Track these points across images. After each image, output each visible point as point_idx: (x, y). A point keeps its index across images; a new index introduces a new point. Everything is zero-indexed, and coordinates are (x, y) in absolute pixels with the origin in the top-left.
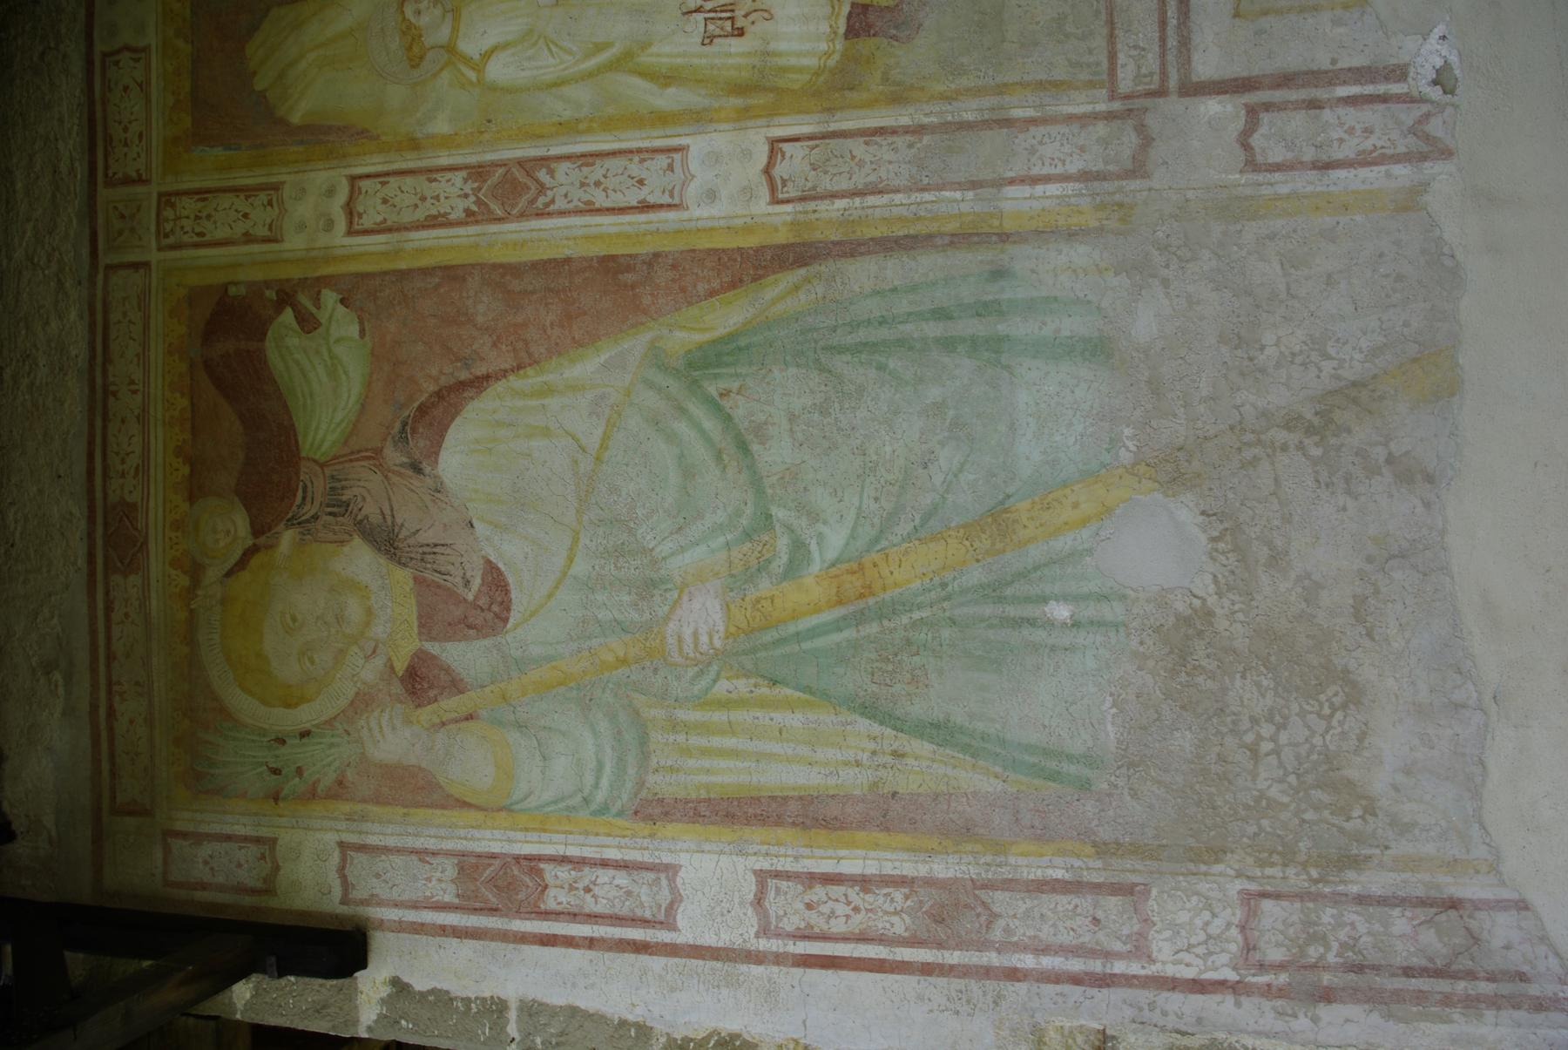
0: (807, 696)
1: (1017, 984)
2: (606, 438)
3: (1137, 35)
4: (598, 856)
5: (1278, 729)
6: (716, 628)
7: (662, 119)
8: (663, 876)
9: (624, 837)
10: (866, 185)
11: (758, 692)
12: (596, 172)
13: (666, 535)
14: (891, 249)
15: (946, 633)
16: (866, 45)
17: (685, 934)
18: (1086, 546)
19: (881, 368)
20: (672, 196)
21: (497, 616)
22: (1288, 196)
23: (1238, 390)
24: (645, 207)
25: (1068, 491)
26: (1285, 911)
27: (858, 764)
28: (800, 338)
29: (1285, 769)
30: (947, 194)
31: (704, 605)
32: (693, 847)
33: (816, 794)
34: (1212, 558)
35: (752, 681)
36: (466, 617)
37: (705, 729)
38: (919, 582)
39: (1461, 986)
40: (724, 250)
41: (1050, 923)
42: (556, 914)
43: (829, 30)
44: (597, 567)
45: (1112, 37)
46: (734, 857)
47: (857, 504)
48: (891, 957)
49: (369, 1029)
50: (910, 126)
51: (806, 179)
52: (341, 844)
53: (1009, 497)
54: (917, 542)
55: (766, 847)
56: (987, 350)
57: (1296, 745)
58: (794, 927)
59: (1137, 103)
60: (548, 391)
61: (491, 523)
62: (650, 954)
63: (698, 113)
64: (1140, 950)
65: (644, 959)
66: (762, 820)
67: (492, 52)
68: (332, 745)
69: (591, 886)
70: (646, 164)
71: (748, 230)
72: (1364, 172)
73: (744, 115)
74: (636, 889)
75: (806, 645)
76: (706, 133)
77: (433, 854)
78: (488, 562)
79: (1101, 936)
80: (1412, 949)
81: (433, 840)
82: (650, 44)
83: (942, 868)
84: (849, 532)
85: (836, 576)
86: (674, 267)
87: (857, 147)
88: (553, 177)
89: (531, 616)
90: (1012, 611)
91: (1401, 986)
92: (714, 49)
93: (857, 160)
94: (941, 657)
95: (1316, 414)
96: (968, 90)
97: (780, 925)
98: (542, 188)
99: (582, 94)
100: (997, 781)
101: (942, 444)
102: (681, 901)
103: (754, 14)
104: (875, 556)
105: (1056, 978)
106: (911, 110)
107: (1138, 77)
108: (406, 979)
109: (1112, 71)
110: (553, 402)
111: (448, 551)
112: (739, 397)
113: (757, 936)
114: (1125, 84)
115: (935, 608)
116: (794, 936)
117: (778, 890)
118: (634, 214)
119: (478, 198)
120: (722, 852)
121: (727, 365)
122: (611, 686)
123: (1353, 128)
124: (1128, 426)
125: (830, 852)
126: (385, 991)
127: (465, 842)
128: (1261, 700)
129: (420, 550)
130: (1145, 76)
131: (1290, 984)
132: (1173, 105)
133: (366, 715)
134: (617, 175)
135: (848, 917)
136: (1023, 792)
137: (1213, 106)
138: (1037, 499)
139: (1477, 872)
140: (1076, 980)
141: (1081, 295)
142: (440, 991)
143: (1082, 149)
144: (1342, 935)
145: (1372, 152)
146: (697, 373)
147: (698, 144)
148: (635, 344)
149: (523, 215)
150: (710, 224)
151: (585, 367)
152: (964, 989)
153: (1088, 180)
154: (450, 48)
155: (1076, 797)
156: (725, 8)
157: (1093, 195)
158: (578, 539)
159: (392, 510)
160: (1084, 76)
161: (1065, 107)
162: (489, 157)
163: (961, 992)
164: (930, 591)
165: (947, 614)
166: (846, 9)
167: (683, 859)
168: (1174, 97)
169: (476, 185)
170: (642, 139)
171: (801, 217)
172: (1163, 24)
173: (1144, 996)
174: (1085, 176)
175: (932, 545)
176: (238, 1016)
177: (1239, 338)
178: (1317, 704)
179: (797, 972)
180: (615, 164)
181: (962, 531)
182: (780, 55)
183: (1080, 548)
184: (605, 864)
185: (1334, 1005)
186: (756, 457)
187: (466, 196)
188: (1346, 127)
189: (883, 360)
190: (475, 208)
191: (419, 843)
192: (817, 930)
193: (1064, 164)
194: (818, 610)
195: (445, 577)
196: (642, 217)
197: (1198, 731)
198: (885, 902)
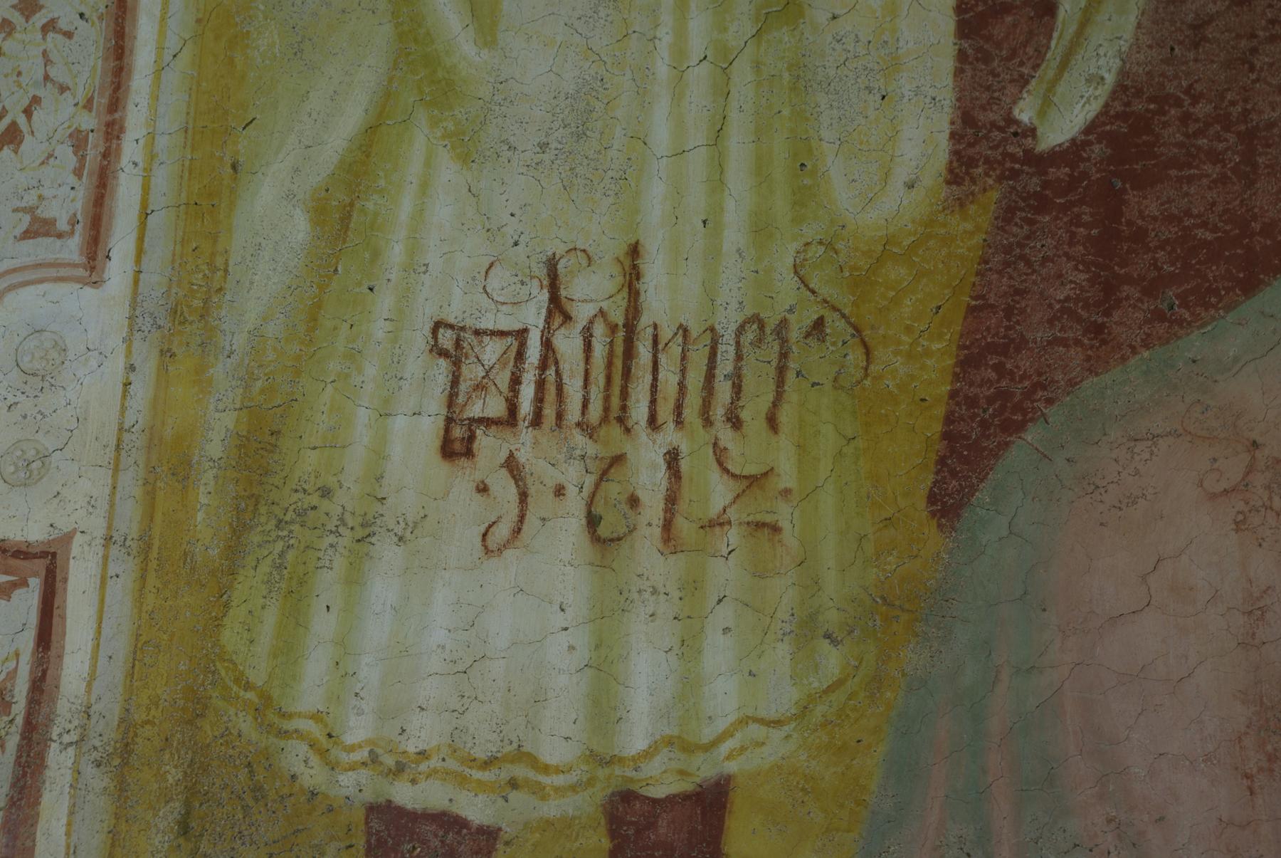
70: (67, 155)
76: (128, 341)
82: (466, 159)
103: (512, 492)
170: (151, 136)
182: (355, 579)
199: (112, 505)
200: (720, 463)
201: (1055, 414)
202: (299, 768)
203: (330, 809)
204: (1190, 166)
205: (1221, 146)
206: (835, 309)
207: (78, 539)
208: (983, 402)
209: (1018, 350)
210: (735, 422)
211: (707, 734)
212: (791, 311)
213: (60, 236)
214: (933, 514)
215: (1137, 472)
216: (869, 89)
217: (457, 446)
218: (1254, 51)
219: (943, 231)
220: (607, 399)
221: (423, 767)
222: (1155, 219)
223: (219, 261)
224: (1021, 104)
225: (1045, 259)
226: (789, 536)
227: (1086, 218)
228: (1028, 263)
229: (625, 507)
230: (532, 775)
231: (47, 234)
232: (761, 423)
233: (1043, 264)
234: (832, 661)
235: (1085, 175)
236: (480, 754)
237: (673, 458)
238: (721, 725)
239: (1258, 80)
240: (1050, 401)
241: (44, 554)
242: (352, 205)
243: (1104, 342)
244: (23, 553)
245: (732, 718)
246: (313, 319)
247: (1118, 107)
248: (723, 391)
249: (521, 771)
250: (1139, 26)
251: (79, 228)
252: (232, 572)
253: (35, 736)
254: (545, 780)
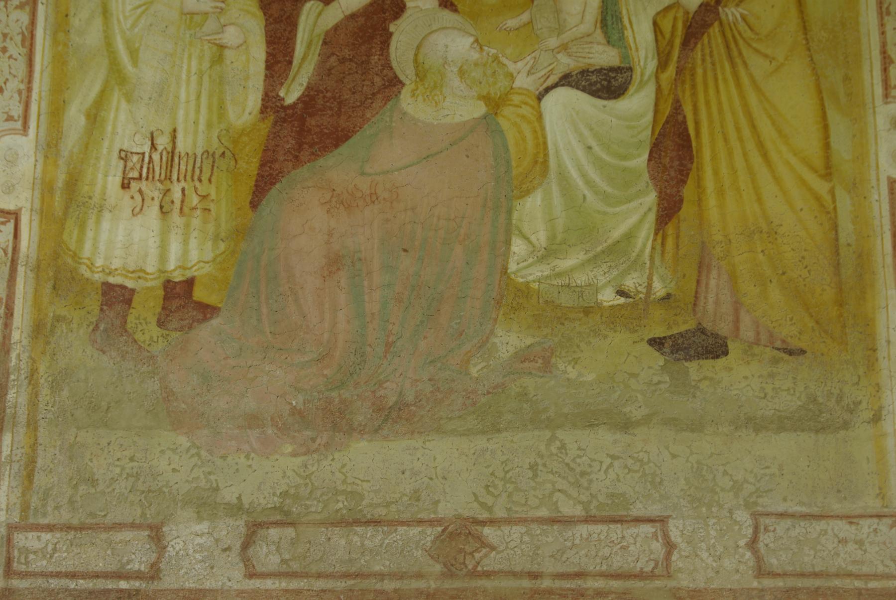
3: (65, 552)
7: (57, 111)
16: (93, 303)
43: (113, 267)
45: (68, 528)
50: (10, 340)
63: (56, 146)
70: (16, 96)
73: (46, 188)
76: (35, 153)
82: (129, 101)
88: (17, 7)
92: (115, 161)
96: (37, 396)
99: (93, 37)
106: (25, 342)
107: (26, 551)
114: (21, 539)
130: (26, 558)
134: (10, 67)
160: (35, 501)
161: (7, 483)
166: (130, 284)
170: (40, 92)
172: (73, 576)
180: (20, 67)
182: (98, 222)
199: (32, 200)
200: (196, 192)
201: (284, 180)
202: (84, 272)
203: (92, 283)
204: (324, 111)
205: (333, 105)
206: (228, 149)
207: (24, 210)
208: (265, 177)
209: (275, 162)
210: (200, 180)
211: (190, 265)
212: (216, 149)
213: (15, 121)
214: (251, 207)
215: (303, 197)
216: (240, 85)
217: (126, 185)
218: (344, 77)
219: (258, 127)
220: (166, 173)
221: (116, 273)
222: (314, 126)
223: (60, 130)
224: (281, 91)
225: (285, 136)
226: (213, 213)
227: (296, 125)
228: (280, 137)
229: (170, 204)
230: (144, 275)
231: (12, 120)
232: (207, 181)
233: (284, 138)
234: (222, 246)
235: (296, 113)
236: (131, 270)
237: (183, 190)
238: (193, 263)
239: (344, 86)
240: (283, 177)
241: (14, 213)
242: (97, 114)
243: (298, 161)
244: (9, 213)
245: (196, 261)
246: (87, 148)
247: (307, 93)
248: (197, 171)
249: (141, 274)
250: (314, 69)
251: (21, 119)
252: (65, 220)
253: (14, 263)
254: (147, 276)
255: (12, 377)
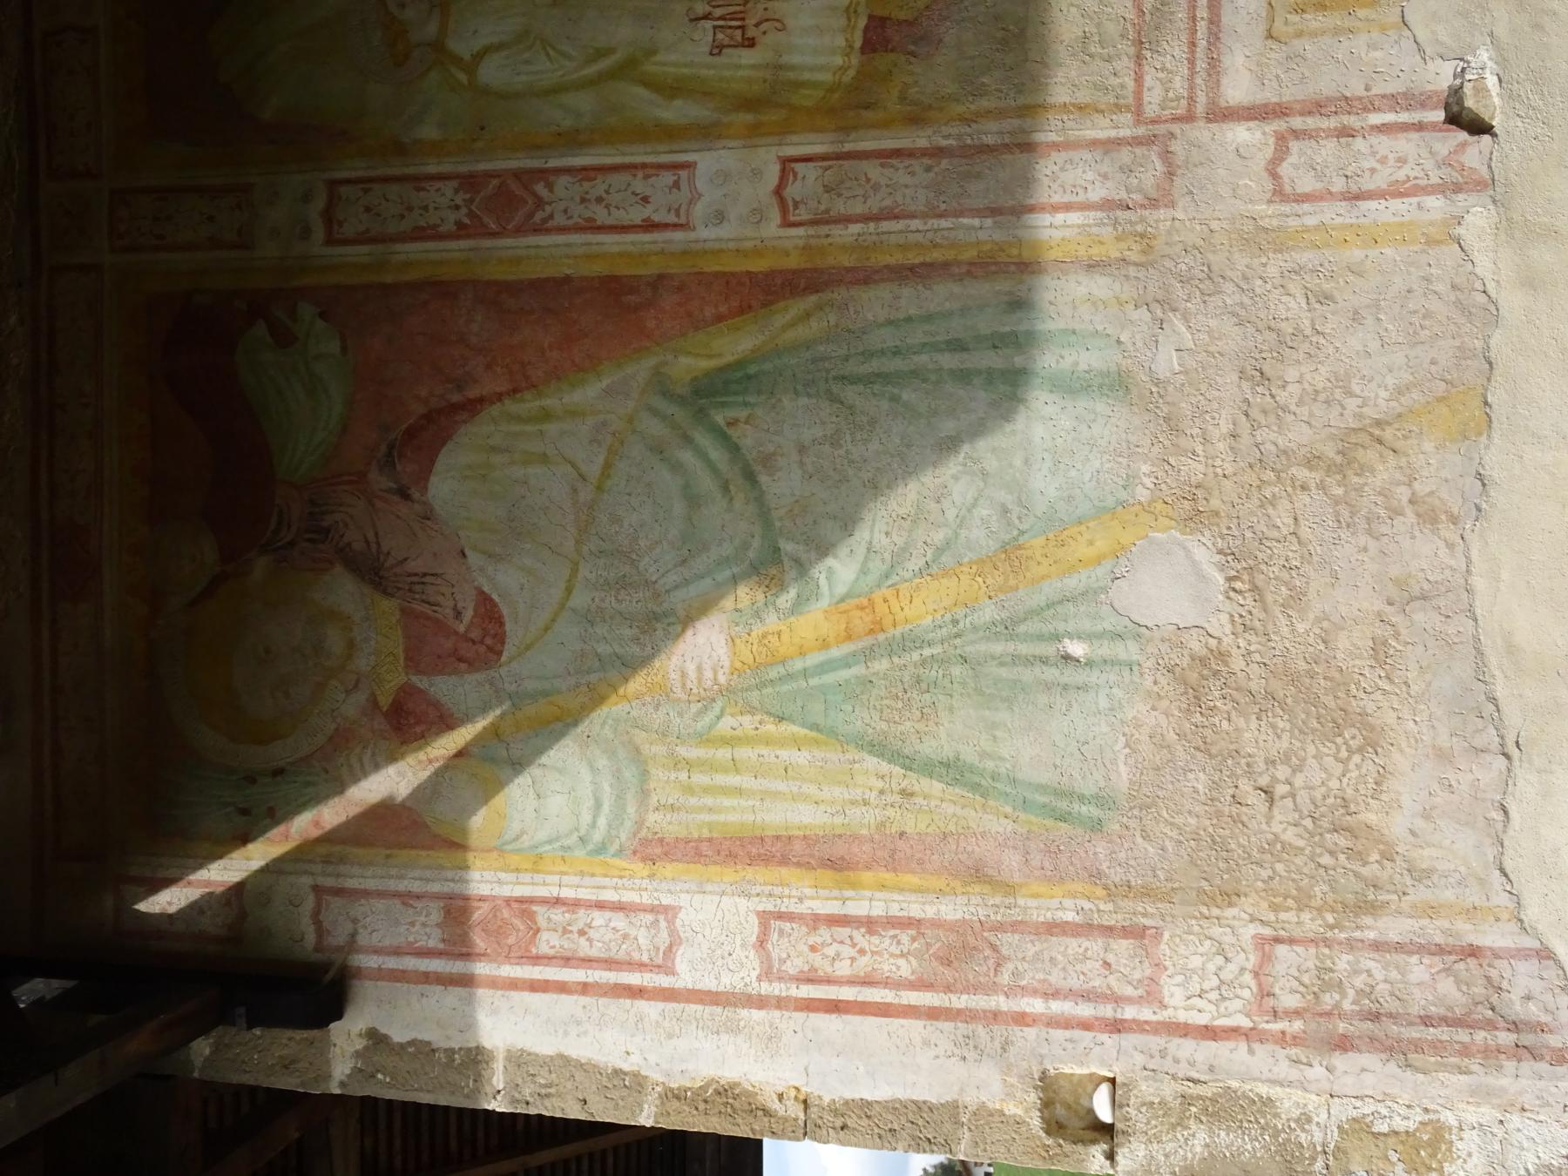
0: (814, 734)
1: (1025, 1029)
2: (607, 466)
4: (594, 898)
5: (1294, 771)
6: (721, 664)
8: (661, 918)
9: (621, 877)
10: (882, 210)
11: (763, 729)
12: (599, 187)
13: (670, 566)
14: (907, 277)
15: (957, 671)
16: (883, 61)
17: (686, 976)
18: (1101, 584)
19: (894, 399)
20: (678, 215)
21: (490, 649)
22: (1316, 228)
23: (1260, 427)
24: (650, 226)
25: (1083, 528)
26: (1299, 956)
27: (866, 803)
28: (811, 367)
29: (1301, 811)
30: (965, 221)
31: (708, 639)
32: (694, 887)
33: (821, 833)
34: (1228, 598)
35: (758, 718)
36: (456, 650)
37: (710, 766)
38: (930, 618)
39: (1480, 1036)
40: (733, 274)
41: (1060, 966)
42: (549, 958)
43: (844, 44)
44: (597, 600)
46: (737, 899)
47: (868, 538)
48: (896, 1001)
49: (342, 1084)
50: (927, 148)
51: (819, 202)
52: (316, 889)
53: (1022, 533)
54: (929, 578)
55: (770, 887)
56: (1003, 383)
57: (1312, 788)
58: (798, 970)
59: (1161, 129)
60: (546, 416)
61: (484, 553)
62: (648, 999)
64: (1151, 994)
65: (642, 1005)
66: (766, 860)
67: (485, 53)
68: (308, 784)
69: (586, 929)
71: (757, 253)
72: (1396, 204)
73: (755, 132)
74: (633, 932)
75: (814, 682)
76: (715, 150)
77: (418, 897)
78: (481, 593)
79: (1112, 980)
80: (1430, 998)
81: (417, 883)
83: (950, 910)
84: (859, 566)
85: (845, 612)
86: (680, 289)
87: (873, 170)
88: (551, 191)
89: (528, 648)
90: (1024, 649)
91: (1418, 1035)
93: (872, 182)
94: (951, 696)
95: (1339, 452)
97: (783, 968)
98: (540, 203)
99: (584, 102)
100: (1007, 821)
101: (956, 478)
102: (680, 944)
103: (765, 24)
104: (885, 592)
105: (1066, 1023)
106: (929, 132)
108: (383, 1031)
109: (1138, 95)
110: (551, 428)
111: (439, 581)
112: (748, 427)
113: (759, 979)
114: (1151, 110)
115: (946, 645)
116: (797, 980)
117: (781, 932)
118: (637, 233)
119: (470, 210)
120: (723, 893)
121: (736, 393)
122: (610, 722)
123: (1386, 157)
124: (1145, 463)
125: (836, 893)
126: (360, 1044)
127: (452, 885)
128: (1276, 739)
129: (409, 579)
131: (1304, 1032)
132: (1201, 132)
133: (346, 752)
134: (620, 191)
135: (853, 959)
136: (1034, 832)
137: (1242, 134)
138: (1051, 536)
139: (1497, 920)
140: (1086, 1025)
141: (1100, 328)
142: (421, 1041)
143: (1105, 176)
144: (1359, 982)
145: (1404, 182)
146: (704, 401)
147: (707, 162)
148: (640, 370)
149: (519, 231)
150: (717, 246)
151: (588, 393)
152: (971, 1035)
153: (1111, 209)
154: (438, 46)
155: (1087, 838)
156: (735, 16)
157: (1116, 222)
158: (577, 570)
159: (376, 534)
161: (1088, 132)
162: (482, 166)
163: (969, 1038)
164: (940, 627)
165: (958, 651)
166: (862, 22)
167: (684, 900)
168: (1202, 123)
169: (468, 196)
170: (646, 153)
171: (813, 242)
173: (1155, 1042)
174: (1107, 205)
175: (944, 581)
176: (196, 1074)
177: (1262, 373)
178: (1333, 746)
179: (800, 1016)
180: (618, 179)
181: (974, 567)
182: (792, 68)
183: (1095, 586)
184: (600, 906)
185: (1350, 1053)
186: (764, 488)
187: (457, 207)
188: (1378, 157)
189: (896, 391)
190: (466, 221)
191: (402, 886)
192: (821, 973)
193: (1086, 192)
194: (825, 645)
195: (434, 608)
196: (647, 237)
197: (1212, 772)
198: (891, 944)
202: (850, 77)
207: (781, 154)
236: (846, 23)
244: (783, 170)
249: (852, 10)
255: (969, 141)
